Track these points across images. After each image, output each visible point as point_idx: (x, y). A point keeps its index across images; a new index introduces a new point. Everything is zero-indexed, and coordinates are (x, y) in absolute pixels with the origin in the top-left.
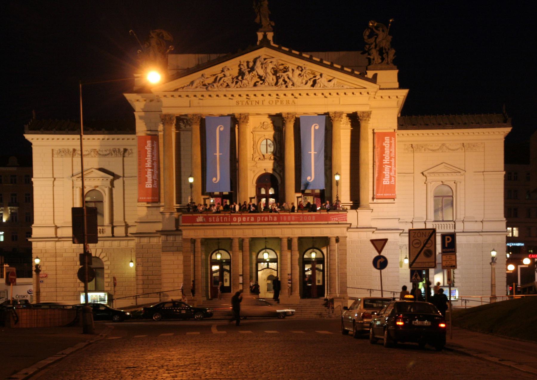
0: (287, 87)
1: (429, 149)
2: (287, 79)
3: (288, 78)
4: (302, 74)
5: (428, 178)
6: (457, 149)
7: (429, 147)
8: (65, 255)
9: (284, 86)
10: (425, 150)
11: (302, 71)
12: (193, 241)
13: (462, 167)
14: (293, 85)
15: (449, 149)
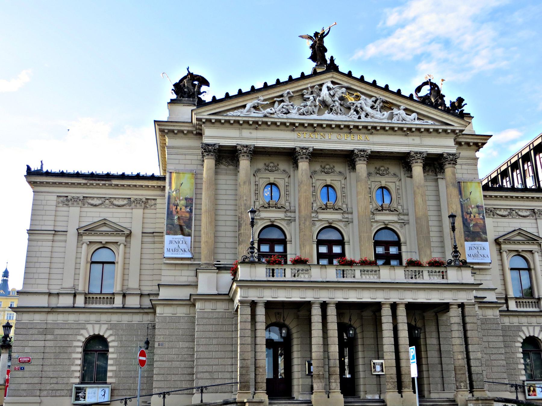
0: (360, 118)
1: (498, 215)
2: (359, 109)
3: (361, 108)
4: (376, 105)
5: (503, 246)
6: (528, 216)
7: (498, 212)
8: (57, 332)
9: (357, 116)
10: (494, 215)
11: (375, 102)
12: (253, 305)
13: (536, 234)
14: (367, 115)
15: (519, 215)
